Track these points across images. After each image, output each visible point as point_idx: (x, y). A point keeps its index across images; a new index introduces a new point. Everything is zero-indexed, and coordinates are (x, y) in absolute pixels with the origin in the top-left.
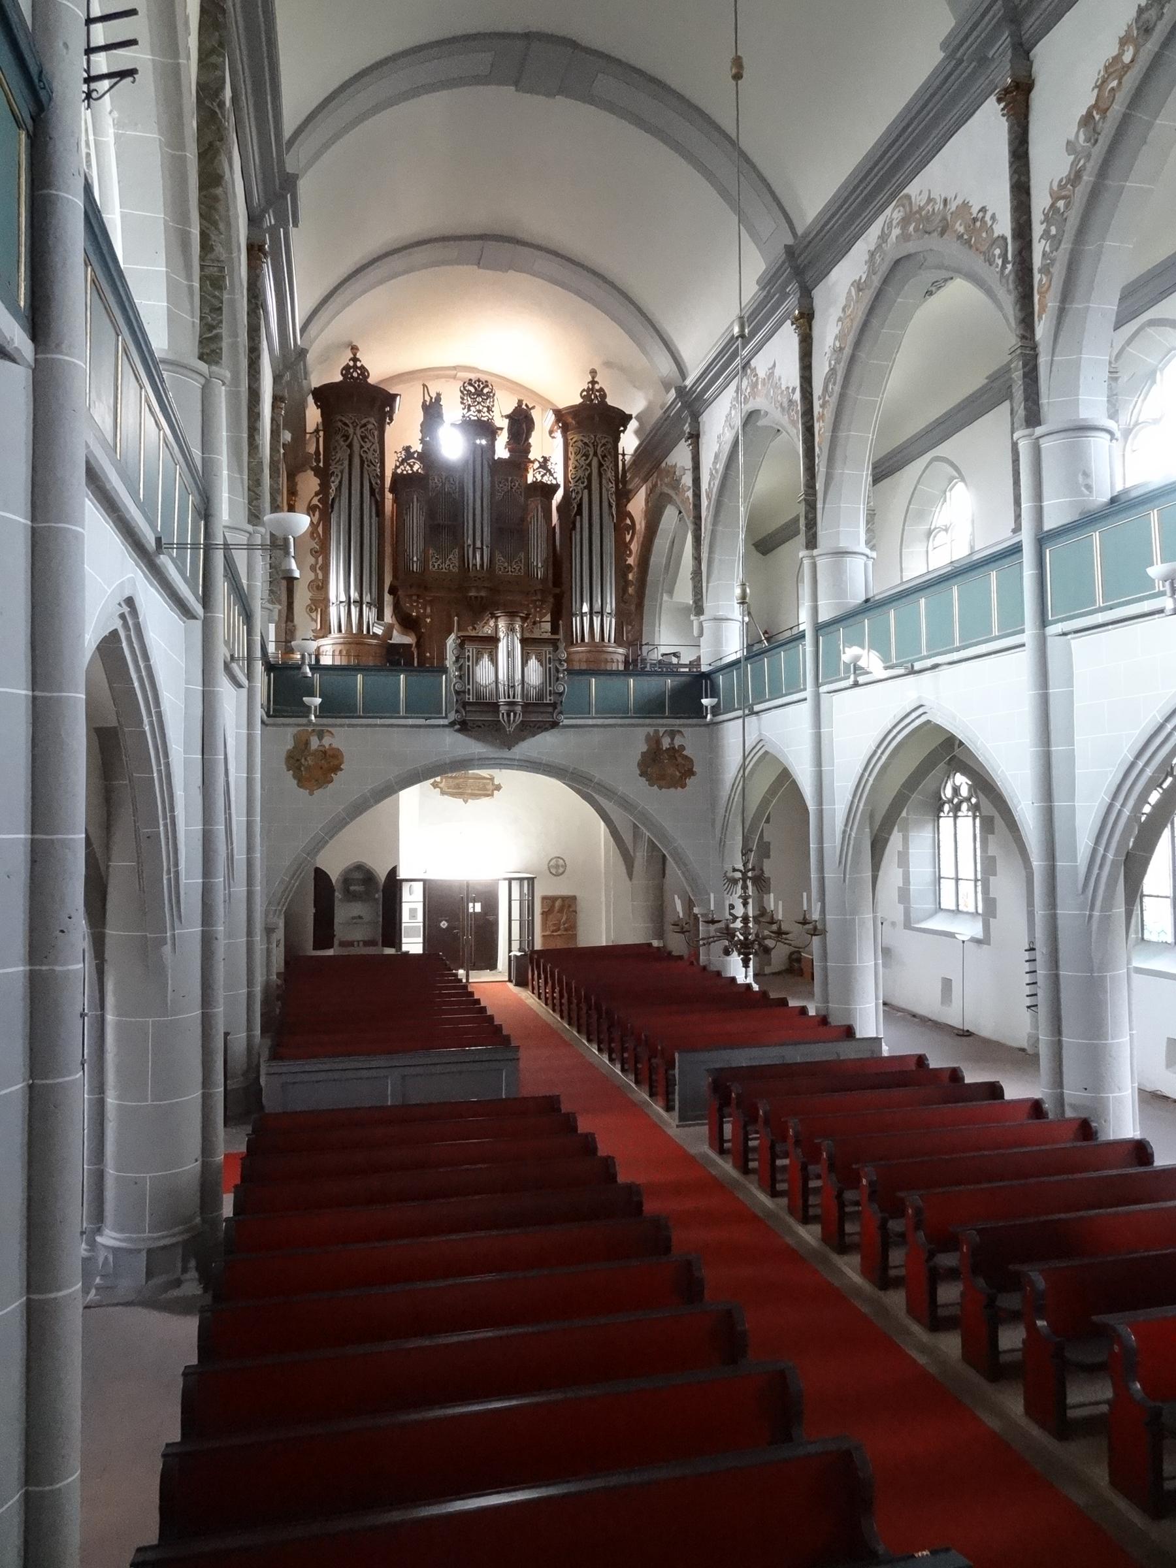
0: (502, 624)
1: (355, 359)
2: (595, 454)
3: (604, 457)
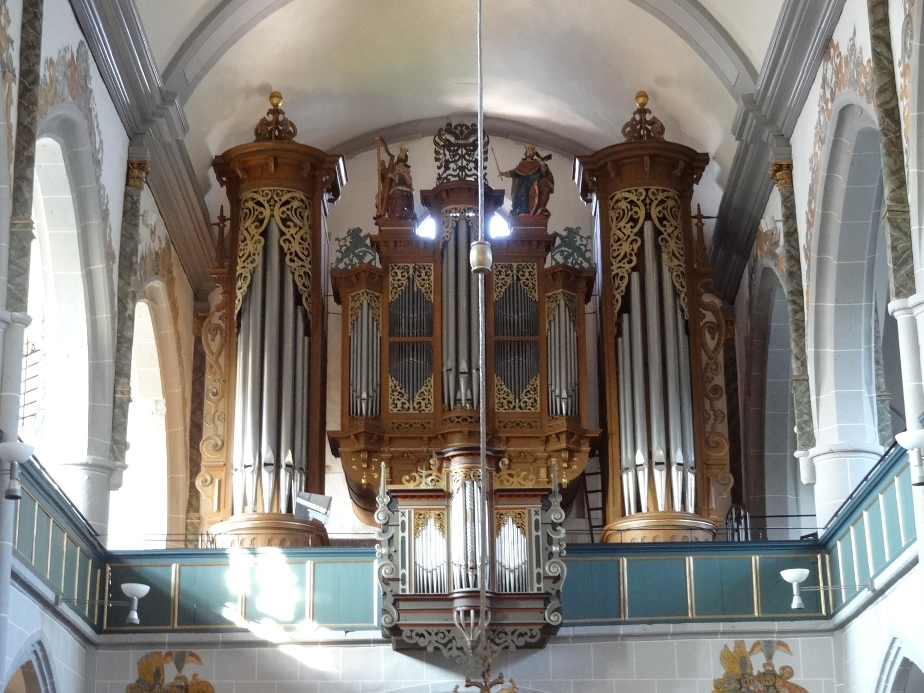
0: (457, 467)
1: (275, 111)
2: (648, 217)
3: (661, 220)
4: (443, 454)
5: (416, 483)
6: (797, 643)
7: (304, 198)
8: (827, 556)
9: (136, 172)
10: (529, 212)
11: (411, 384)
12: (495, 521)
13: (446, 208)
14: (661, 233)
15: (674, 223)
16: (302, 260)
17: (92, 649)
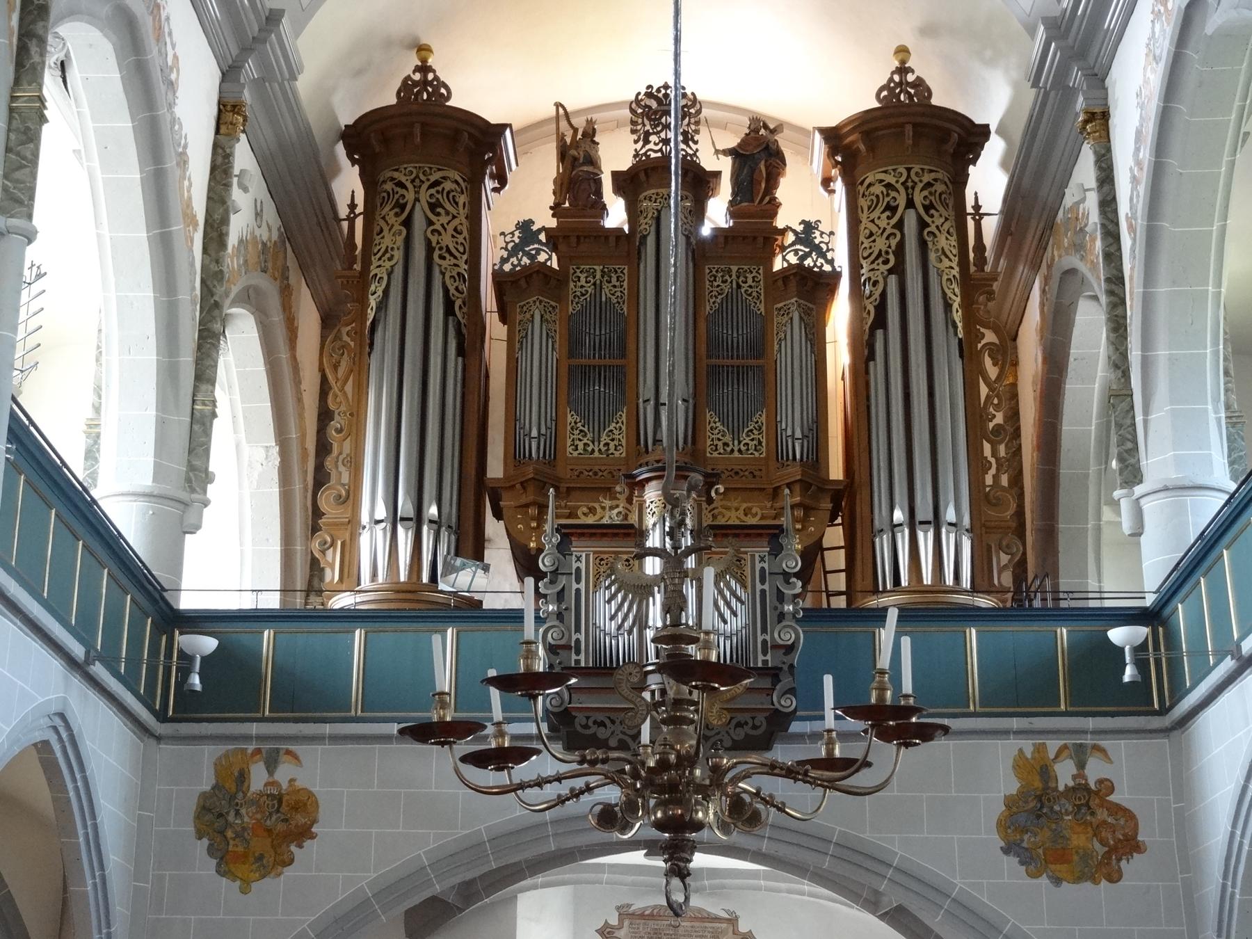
0: (652, 494)
1: (424, 68)
2: (910, 204)
3: (927, 208)
4: (634, 477)
5: (597, 517)
6: (1119, 748)
7: (461, 181)
8: (1161, 629)
9: (229, 116)
10: (753, 201)
11: (597, 421)
14: (928, 225)
15: (945, 213)
16: (455, 258)
17: (153, 742)
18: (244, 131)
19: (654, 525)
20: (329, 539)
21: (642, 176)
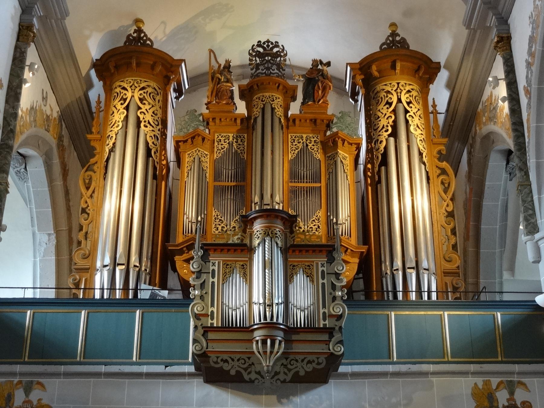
1: (139, 31)
2: (399, 101)
3: (409, 103)
6: (533, 382)
12: (289, 271)
13: (256, 96)
14: (409, 112)
15: (418, 107)
16: (153, 127)
18: (33, 42)
19: (259, 244)
20: (78, 277)
21: (255, 87)
